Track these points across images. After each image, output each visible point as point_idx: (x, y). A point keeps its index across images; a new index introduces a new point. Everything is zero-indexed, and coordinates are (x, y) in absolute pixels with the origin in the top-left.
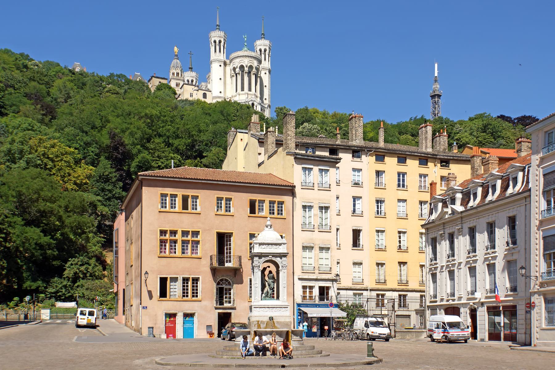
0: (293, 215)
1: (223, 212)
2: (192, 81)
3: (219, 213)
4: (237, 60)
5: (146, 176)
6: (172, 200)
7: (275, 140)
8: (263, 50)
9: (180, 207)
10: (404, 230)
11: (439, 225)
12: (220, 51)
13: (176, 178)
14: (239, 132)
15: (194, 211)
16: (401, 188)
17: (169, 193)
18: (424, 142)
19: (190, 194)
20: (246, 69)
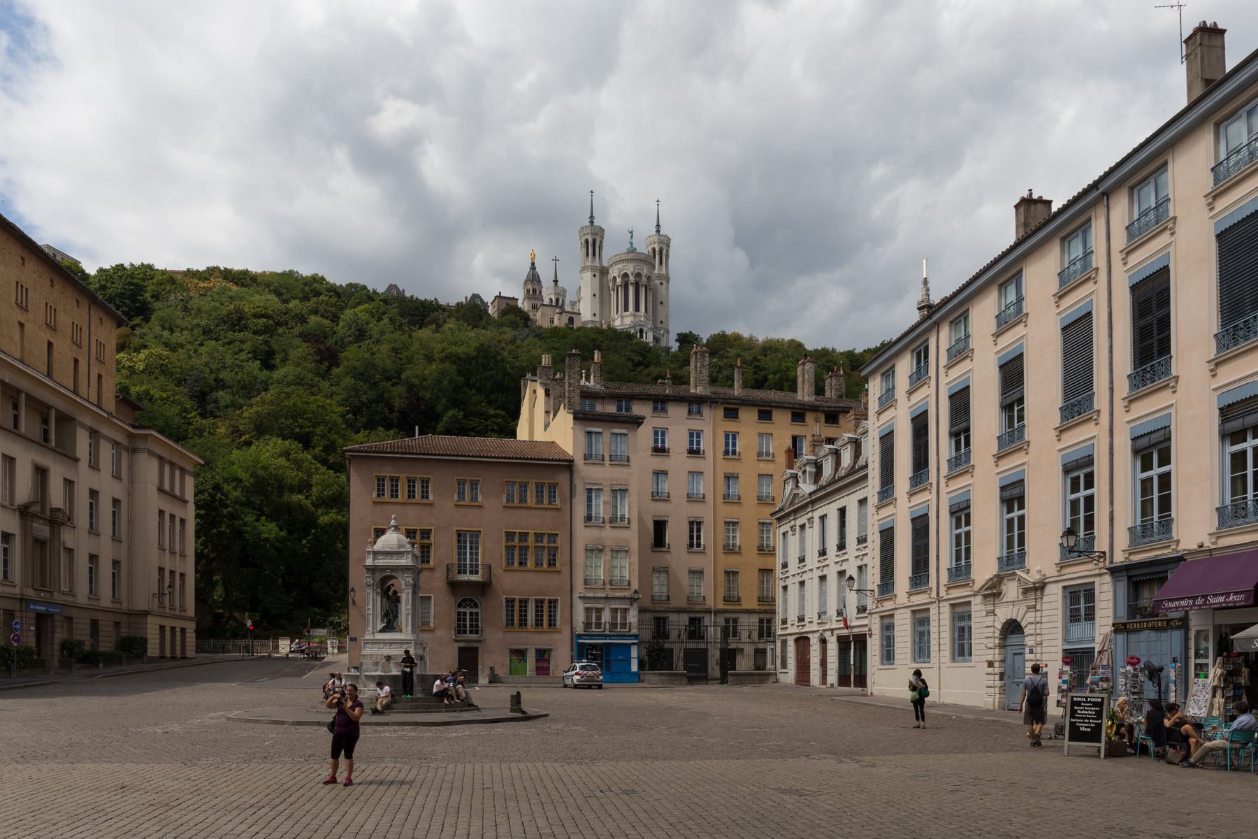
4: (620, 266)
5: (354, 451)
12: (594, 254)
15: (425, 501)
20: (632, 278)
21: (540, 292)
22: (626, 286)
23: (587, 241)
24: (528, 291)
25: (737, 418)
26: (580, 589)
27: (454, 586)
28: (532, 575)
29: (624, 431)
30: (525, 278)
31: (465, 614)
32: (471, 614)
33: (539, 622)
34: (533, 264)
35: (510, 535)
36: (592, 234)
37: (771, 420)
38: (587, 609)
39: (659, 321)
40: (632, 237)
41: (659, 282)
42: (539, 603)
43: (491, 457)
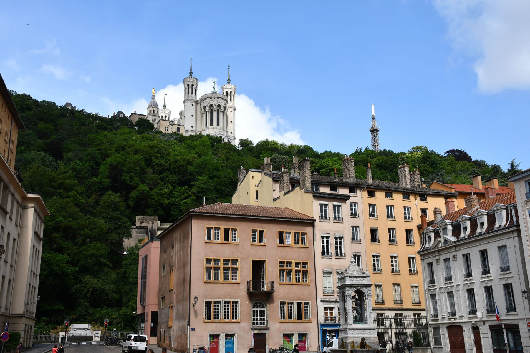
0: (314, 245)
1: (257, 242)
2: (166, 117)
3: (254, 243)
4: (208, 100)
5: (196, 212)
6: (215, 233)
7: (289, 179)
8: (229, 93)
9: (222, 239)
11: (434, 252)
12: (192, 93)
13: (220, 214)
14: (251, 171)
15: (234, 242)
16: (390, 219)
17: (214, 226)
18: (403, 179)
19: (231, 227)
20: (215, 108)
23: (188, 85)
24: (151, 111)
26: (320, 296)
28: (295, 286)
32: (260, 312)
35: (281, 263)
37: (426, 201)
38: (326, 309)
42: (299, 304)
43: (228, 214)
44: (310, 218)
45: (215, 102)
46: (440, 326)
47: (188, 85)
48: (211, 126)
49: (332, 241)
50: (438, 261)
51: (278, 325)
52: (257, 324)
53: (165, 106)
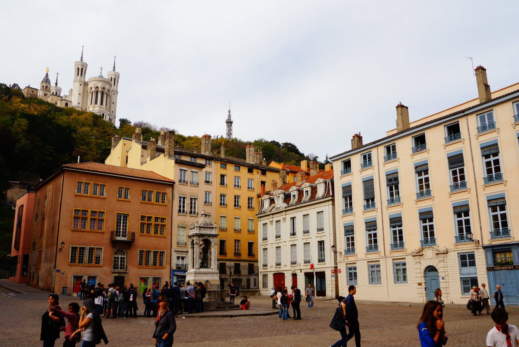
5: (68, 167)
6: (85, 187)
10: (225, 216)
11: (269, 215)
12: (82, 75)
13: (90, 171)
14: (123, 139)
15: (102, 196)
20: (100, 89)
21: (49, 88)
22: (97, 93)
23: (78, 68)
24: (43, 87)
25: (226, 168)
26: (174, 246)
27: (114, 243)
28: (153, 238)
29: (196, 171)
30: (42, 80)
31: (118, 258)
32: (121, 258)
33: (155, 264)
34: (47, 74)
35: (143, 217)
36: (82, 65)
39: (111, 111)
40: (101, 70)
41: (113, 93)
42: (155, 253)
44: (171, 181)
45: (100, 85)
46: (269, 273)
47: (78, 68)
48: (95, 104)
49: (187, 202)
50: (271, 222)
51: (136, 270)
52: (118, 268)
53: (56, 84)
